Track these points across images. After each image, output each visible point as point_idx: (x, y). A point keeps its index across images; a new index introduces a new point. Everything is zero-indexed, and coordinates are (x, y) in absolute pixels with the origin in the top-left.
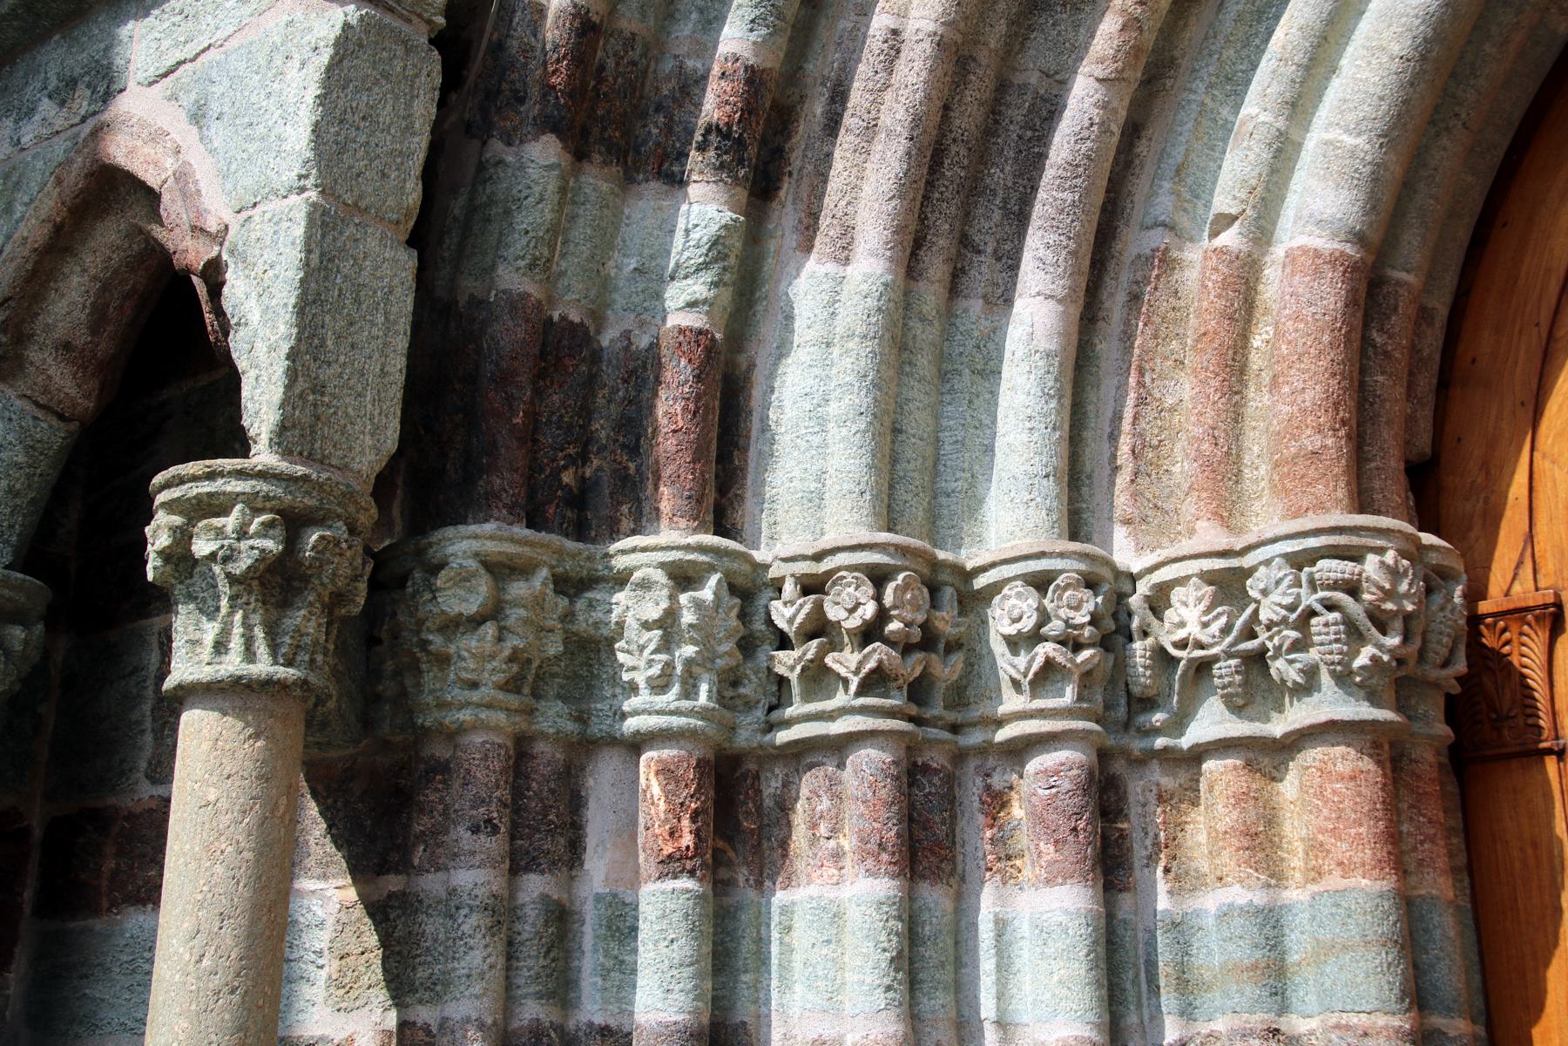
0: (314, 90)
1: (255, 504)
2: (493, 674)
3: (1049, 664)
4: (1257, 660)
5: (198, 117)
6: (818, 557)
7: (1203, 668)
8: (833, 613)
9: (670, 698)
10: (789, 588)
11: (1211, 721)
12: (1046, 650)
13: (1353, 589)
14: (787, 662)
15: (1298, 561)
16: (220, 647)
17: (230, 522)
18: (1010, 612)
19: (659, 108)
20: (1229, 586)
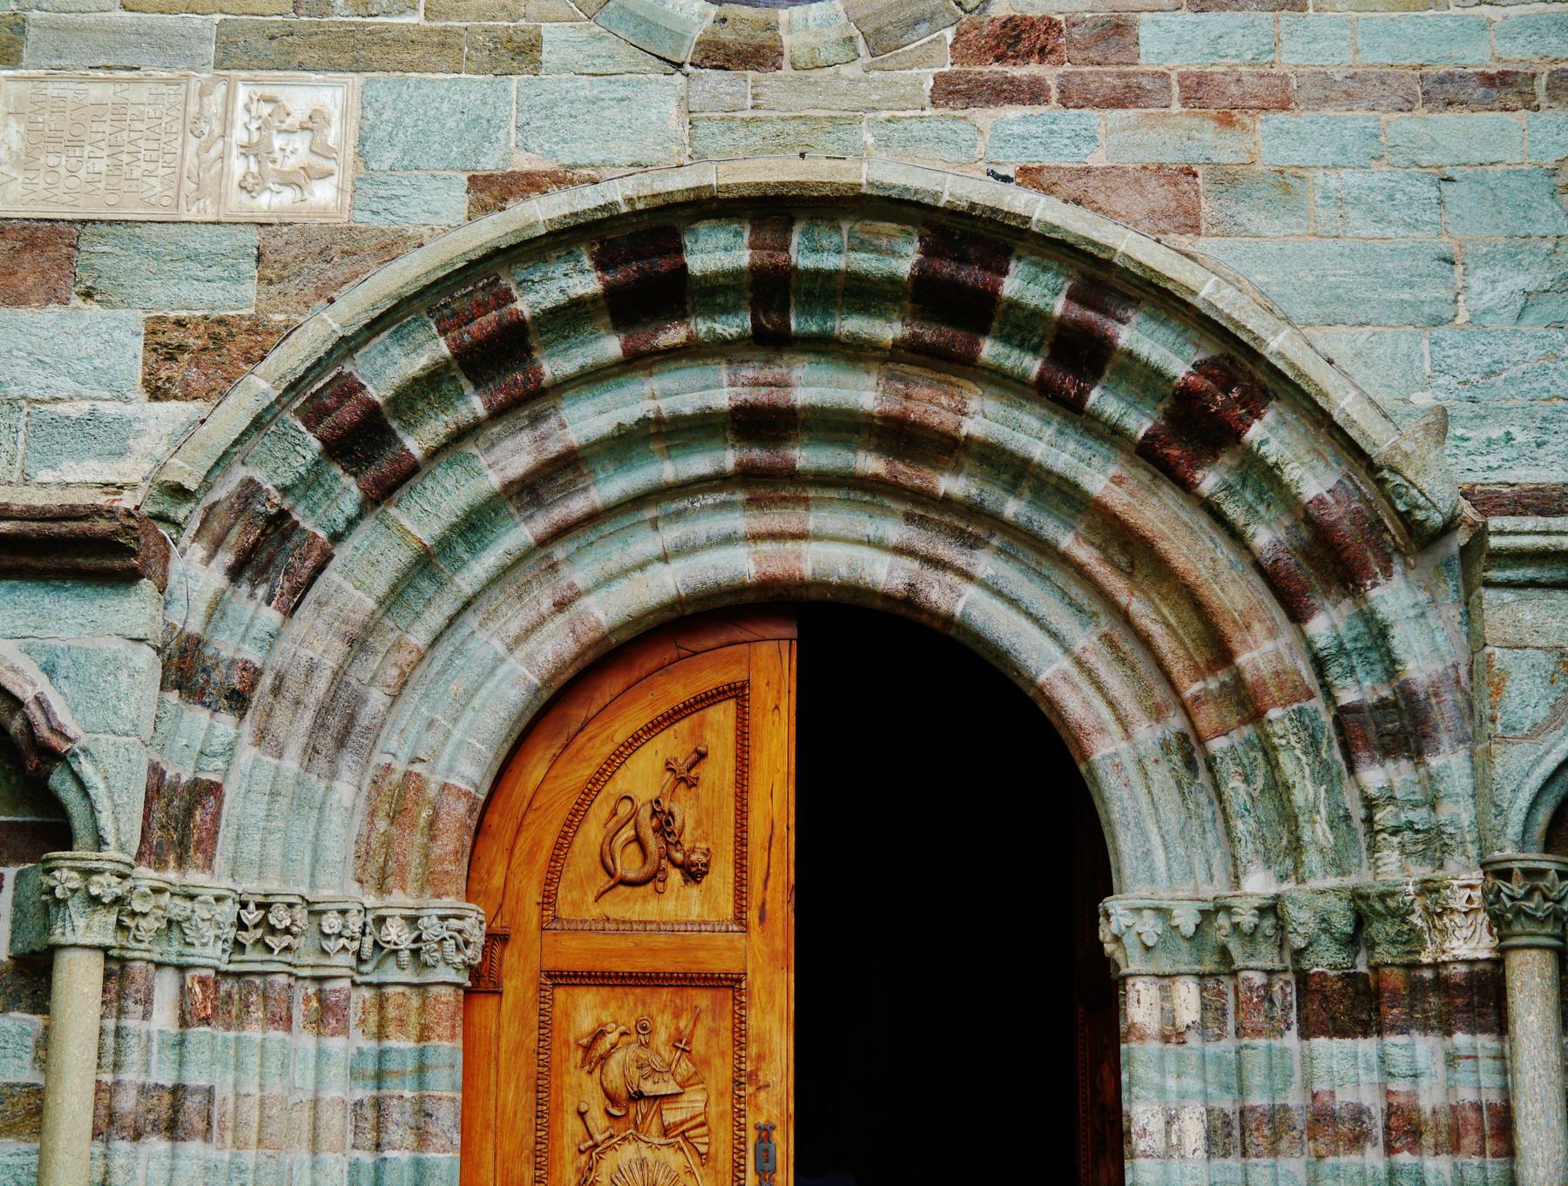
5: (50, 671)
6: (266, 896)
7: (395, 952)
8: (272, 921)
9: (208, 951)
10: (252, 906)
12: (343, 941)
13: (460, 932)
14: (248, 937)
15: (443, 918)
19: (204, 670)
20: (412, 921)
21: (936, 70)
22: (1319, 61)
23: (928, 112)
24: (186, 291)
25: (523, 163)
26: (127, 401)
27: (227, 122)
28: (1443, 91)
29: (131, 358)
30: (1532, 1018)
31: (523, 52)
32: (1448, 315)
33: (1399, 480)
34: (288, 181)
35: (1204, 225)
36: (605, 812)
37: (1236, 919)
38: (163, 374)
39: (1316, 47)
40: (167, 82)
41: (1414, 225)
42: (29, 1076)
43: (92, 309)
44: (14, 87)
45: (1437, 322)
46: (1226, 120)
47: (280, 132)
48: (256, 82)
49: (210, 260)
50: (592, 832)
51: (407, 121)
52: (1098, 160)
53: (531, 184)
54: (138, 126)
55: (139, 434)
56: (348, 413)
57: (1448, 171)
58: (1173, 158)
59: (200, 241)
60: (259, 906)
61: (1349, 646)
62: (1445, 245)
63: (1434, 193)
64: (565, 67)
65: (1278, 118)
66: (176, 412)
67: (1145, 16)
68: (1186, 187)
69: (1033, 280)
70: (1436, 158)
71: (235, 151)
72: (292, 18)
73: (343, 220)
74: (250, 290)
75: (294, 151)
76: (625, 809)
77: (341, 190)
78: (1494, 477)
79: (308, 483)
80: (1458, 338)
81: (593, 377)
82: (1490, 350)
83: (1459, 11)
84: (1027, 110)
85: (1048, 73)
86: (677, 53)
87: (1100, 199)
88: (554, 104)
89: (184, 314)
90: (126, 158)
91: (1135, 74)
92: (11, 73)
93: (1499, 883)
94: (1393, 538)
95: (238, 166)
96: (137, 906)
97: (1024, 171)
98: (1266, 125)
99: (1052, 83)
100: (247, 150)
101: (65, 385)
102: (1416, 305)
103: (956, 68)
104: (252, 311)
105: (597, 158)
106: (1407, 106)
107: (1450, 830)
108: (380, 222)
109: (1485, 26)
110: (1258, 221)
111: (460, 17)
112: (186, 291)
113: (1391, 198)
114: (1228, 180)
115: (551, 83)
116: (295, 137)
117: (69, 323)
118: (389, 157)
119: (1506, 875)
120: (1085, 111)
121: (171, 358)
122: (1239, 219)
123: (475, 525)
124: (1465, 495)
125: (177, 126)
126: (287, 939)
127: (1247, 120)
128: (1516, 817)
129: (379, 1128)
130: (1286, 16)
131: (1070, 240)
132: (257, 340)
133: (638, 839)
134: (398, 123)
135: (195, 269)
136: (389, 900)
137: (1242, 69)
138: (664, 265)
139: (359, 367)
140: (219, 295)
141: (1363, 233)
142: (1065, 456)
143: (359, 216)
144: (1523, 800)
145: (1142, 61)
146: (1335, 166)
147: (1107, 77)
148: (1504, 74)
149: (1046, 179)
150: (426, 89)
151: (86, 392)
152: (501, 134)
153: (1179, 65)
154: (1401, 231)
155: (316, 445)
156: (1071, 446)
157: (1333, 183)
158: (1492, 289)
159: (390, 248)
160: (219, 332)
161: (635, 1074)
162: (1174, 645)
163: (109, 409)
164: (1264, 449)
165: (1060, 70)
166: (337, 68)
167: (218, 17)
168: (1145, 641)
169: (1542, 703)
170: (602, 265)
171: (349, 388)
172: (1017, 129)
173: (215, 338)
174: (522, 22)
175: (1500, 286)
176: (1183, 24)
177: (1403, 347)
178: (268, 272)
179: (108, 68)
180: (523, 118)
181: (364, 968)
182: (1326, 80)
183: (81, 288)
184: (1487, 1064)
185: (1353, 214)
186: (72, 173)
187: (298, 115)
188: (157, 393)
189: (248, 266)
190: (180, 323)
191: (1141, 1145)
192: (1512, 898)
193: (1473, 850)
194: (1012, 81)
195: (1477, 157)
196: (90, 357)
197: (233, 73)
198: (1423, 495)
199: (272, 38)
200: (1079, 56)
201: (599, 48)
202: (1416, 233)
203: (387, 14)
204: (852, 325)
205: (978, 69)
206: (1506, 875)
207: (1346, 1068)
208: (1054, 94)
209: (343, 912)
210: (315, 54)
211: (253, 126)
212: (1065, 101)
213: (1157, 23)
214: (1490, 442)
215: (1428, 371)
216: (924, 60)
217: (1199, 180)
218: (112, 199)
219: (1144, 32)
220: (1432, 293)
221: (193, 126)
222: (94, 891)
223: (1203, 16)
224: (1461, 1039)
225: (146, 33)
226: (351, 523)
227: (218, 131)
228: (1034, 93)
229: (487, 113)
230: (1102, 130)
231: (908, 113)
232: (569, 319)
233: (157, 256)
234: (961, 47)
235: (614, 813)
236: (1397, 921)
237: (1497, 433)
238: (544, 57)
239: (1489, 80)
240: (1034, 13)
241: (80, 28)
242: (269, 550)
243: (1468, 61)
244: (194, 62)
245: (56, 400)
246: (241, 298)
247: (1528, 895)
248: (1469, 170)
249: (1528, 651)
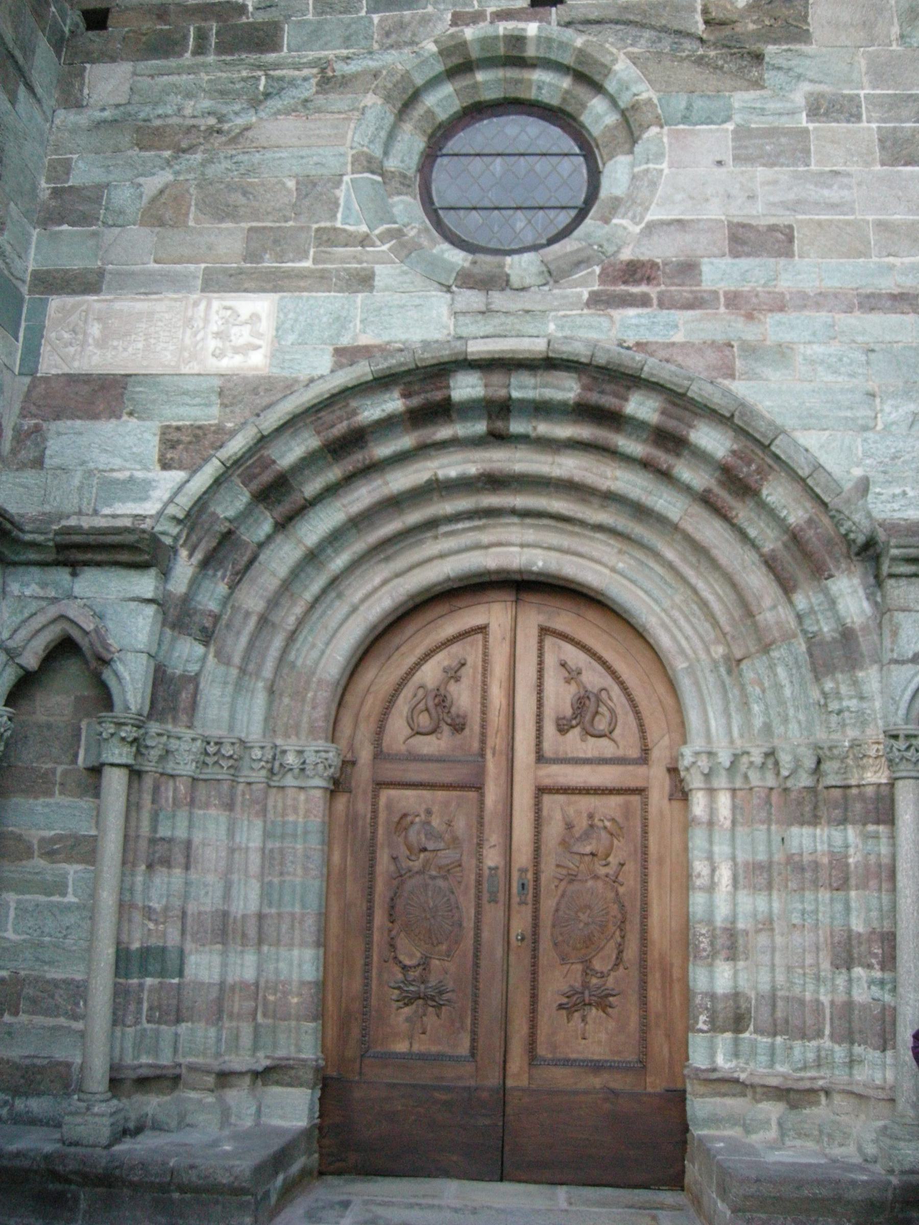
0: (148, 629)
1: (133, 725)
2: (155, 759)
3: (263, 767)
4: (303, 770)
7: (291, 770)
9: (188, 767)
11: (289, 780)
12: (263, 763)
14: (210, 760)
15: (317, 752)
16: (121, 755)
17: (128, 728)
18: (257, 753)
20: (300, 752)
21: (590, 289)
22: (801, 285)
23: (586, 311)
24: (182, 411)
25: (365, 340)
26: (149, 470)
27: (206, 320)
28: (870, 302)
29: (152, 446)
31: (363, 281)
32: (871, 425)
33: (842, 516)
34: (237, 350)
35: (737, 374)
36: (410, 695)
37: (752, 759)
38: (169, 456)
39: (799, 277)
40: (176, 300)
41: (852, 375)
42: (93, 832)
43: (133, 422)
44: (97, 306)
45: (865, 428)
46: (750, 317)
47: (234, 325)
48: (222, 299)
49: (194, 394)
50: (402, 706)
51: (301, 318)
52: (679, 337)
53: (366, 352)
54: (160, 324)
55: (155, 488)
56: (266, 477)
57: (872, 346)
58: (720, 338)
59: (190, 385)
60: (216, 743)
61: (816, 608)
62: (872, 386)
63: (864, 358)
64: (386, 289)
65: (778, 316)
66: (178, 476)
67: (706, 260)
68: (727, 353)
69: (641, 404)
70: (866, 339)
71: (210, 336)
72: (243, 265)
73: (265, 372)
74: (215, 410)
75: (241, 335)
76: (421, 693)
77: (265, 356)
78: (897, 515)
79: (245, 515)
80: (877, 438)
81: (401, 458)
82: (895, 444)
83: (877, 259)
84: (639, 311)
85: (651, 291)
86: (448, 280)
87: (680, 359)
88: (381, 308)
89: (181, 423)
90: (153, 341)
91: (700, 291)
92: (96, 298)
95: (213, 344)
96: (149, 743)
97: (638, 344)
98: (771, 319)
99: (654, 296)
100: (218, 335)
101: (117, 462)
102: (854, 419)
103: (601, 288)
104: (216, 422)
105: (403, 337)
106: (849, 310)
107: (868, 711)
108: (285, 373)
109: (891, 267)
110: (768, 372)
111: (332, 263)
112: (182, 411)
113: (841, 360)
114: (751, 350)
115: (378, 296)
116: (242, 328)
117: (120, 429)
118: (291, 338)
119: (895, 737)
120: (672, 311)
121: (173, 447)
122: (758, 370)
123: (335, 538)
124: (880, 525)
125: (180, 323)
126: (231, 762)
127: (762, 317)
128: (903, 705)
129: (282, 864)
130: (782, 261)
131: (662, 382)
132: (221, 435)
133: (427, 710)
134: (296, 320)
135: (187, 399)
136: (290, 741)
137: (759, 289)
138: (438, 396)
139: (272, 452)
140: (199, 413)
141: (825, 379)
142: (661, 501)
143: (275, 370)
144: (907, 696)
145: (703, 284)
146: (810, 342)
147: (685, 291)
148: (903, 294)
149: (651, 348)
150: (312, 302)
151: (128, 465)
152: (351, 325)
153: (723, 286)
154: (846, 379)
155: (248, 494)
156: (665, 495)
157: (809, 352)
158: (894, 412)
159: (290, 387)
160: (198, 433)
161: (423, 836)
163: (139, 475)
164: (769, 498)
165: (658, 289)
166: (264, 290)
167: (203, 266)
168: (704, 604)
170: (406, 395)
171: (269, 463)
172: (634, 321)
173: (196, 436)
174: (365, 265)
175: (900, 410)
176: (727, 264)
177: (847, 442)
178: (226, 401)
179: (146, 294)
180: (365, 316)
181: (275, 778)
182: (803, 295)
183: (128, 410)
184: (884, 840)
185: (820, 369)
186: (125, 349)
187: (244, 316)
188: (166, 465)
189: (214, 398)
190: (178, 428)
191: (698, 882)
192: (899, 750)
193: (880, 723)
194: (631, 295)
195: (888, 338)
196: (130, 447)
197: (211, 295)
199: (231, 276)
200: (668, 281)
201: (407, 278)
202: (854, 380)
203: (293, 261)
204: (544, 428)
205: (613, 288)
206: (895, 737)
207: (810, 840)
208: (655, 302)
209: (262, 748)
210: (252, 285)
211: (220, 323)
212: (661, 305)
213: (712, 264)
214: (894, 496)
215: (860, 454)
216: (583, 283)
217: (735, 349)
218: (145, 363)
219: (705, 269)
220: (863, 412)
221: (188, 322)
222: (123, 734)
223: (737, 260)
224: (871, 828)
225: (165, 275)
226: (269, 538)
227: (201, 325)
228: (643, 301)
229: (344, 313)
230: (681, 322)
231: (574, 312)
232: (388, 424)
233: (167, 393)
234: (604, 277)
235: (415, 695)
237: (898, 491)
238: (376, 283)
239: (894, 297)
240: (642, 258)
241: (133, 274)
242: (225, 552)
243: (883, 286)
244: (190, 290)
245: (112, 470)
246: (210, 415)
247: (908, 748)
248: (884, 346)
249: (913, 614)
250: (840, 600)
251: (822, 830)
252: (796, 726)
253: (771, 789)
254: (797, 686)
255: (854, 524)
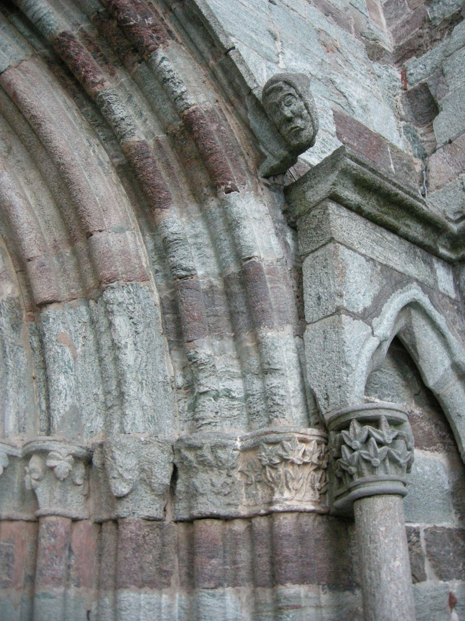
30: (398, 563)
33: (292, 91)
37: (51, 463)
93: (368, 428)
94: (246, 162)
107: (282, 392)
162: (31, 219)
169: (367, 294)
192: (380, 444)
198: (307, 108)
236: (224, 472)
250: (244, 223)
251: (172, 596)
252: (139, 413)
253: (75, 520)
254: (143, 352)
255: (306, 106)
